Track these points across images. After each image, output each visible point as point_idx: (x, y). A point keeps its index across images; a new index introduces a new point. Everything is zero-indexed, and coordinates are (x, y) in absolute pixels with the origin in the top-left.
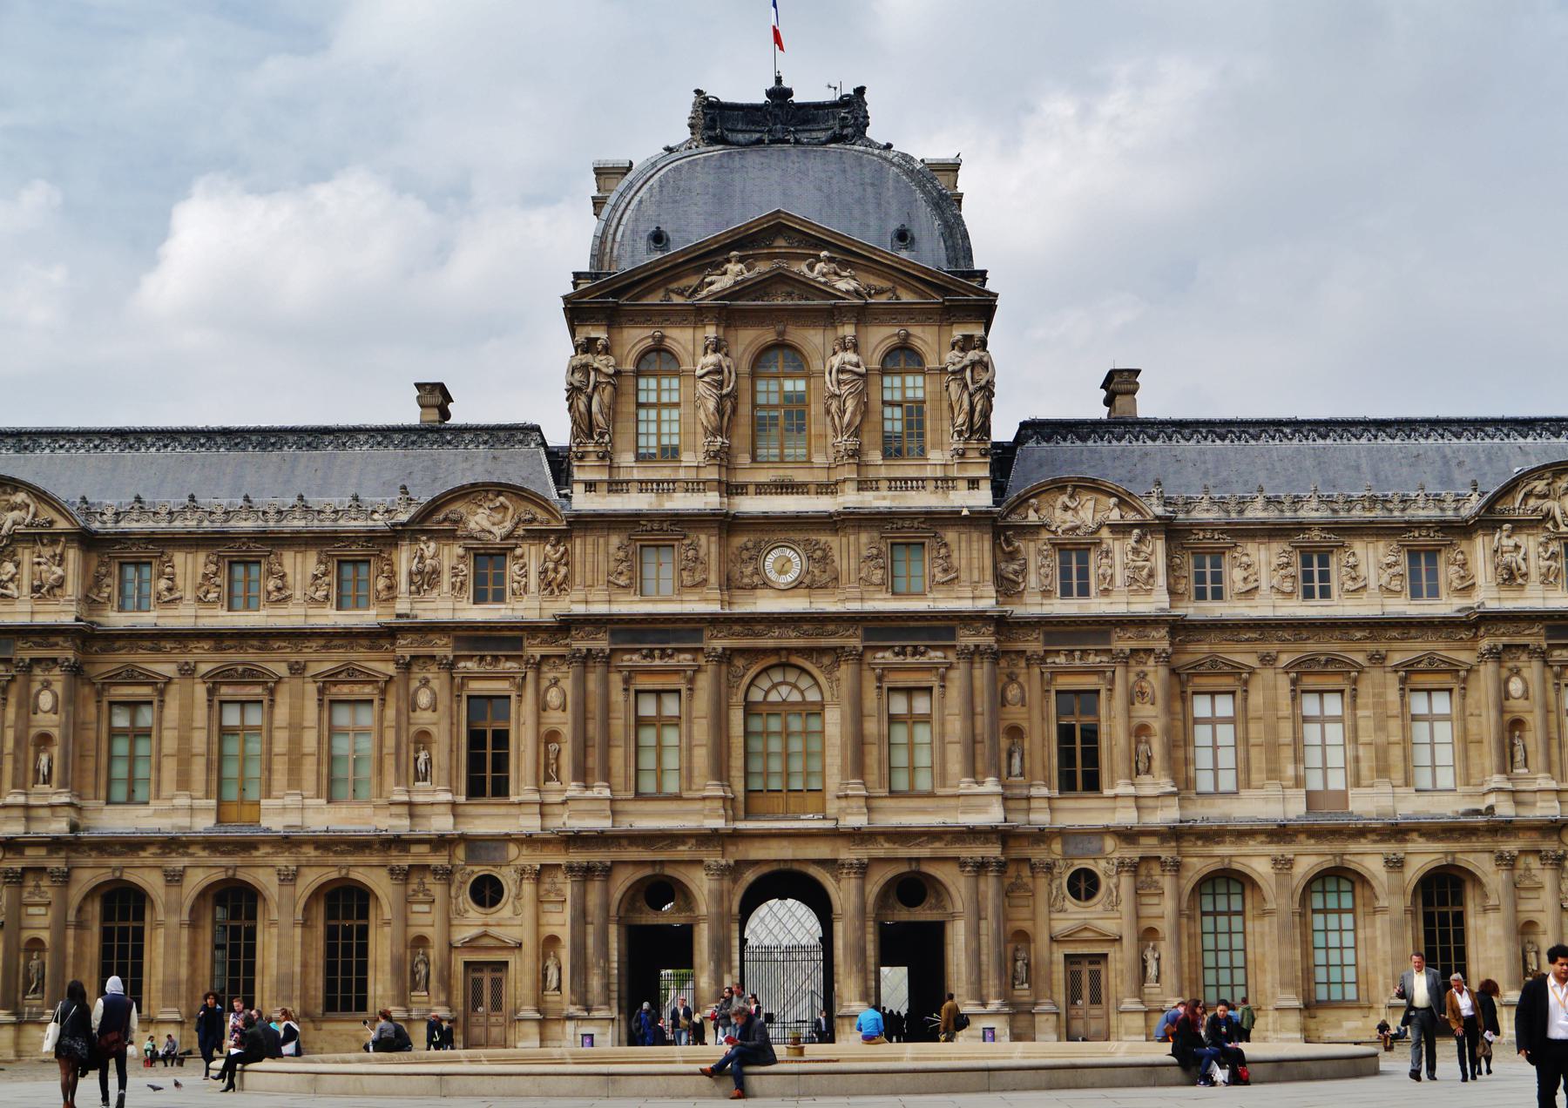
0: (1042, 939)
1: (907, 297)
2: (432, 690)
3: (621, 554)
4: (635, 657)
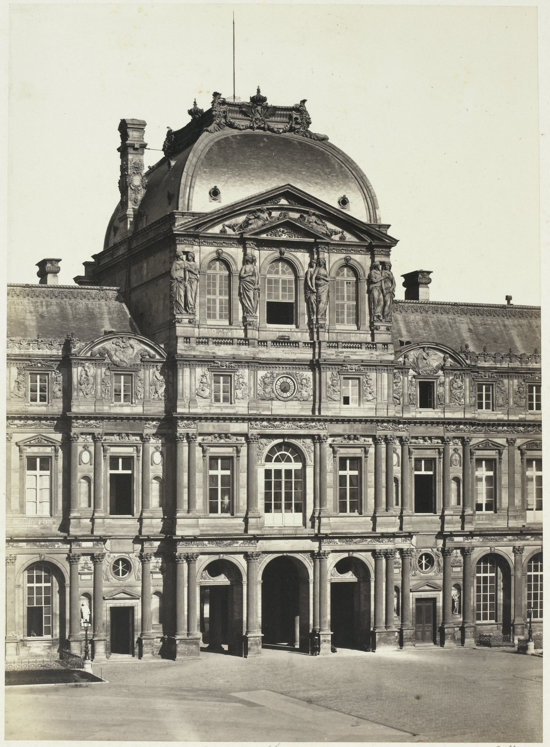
0: (407, 590)
1: (349, 238)
2: (90, 452)
3: (204, 380)
4: (210, 438)
